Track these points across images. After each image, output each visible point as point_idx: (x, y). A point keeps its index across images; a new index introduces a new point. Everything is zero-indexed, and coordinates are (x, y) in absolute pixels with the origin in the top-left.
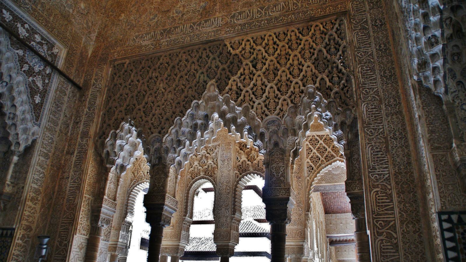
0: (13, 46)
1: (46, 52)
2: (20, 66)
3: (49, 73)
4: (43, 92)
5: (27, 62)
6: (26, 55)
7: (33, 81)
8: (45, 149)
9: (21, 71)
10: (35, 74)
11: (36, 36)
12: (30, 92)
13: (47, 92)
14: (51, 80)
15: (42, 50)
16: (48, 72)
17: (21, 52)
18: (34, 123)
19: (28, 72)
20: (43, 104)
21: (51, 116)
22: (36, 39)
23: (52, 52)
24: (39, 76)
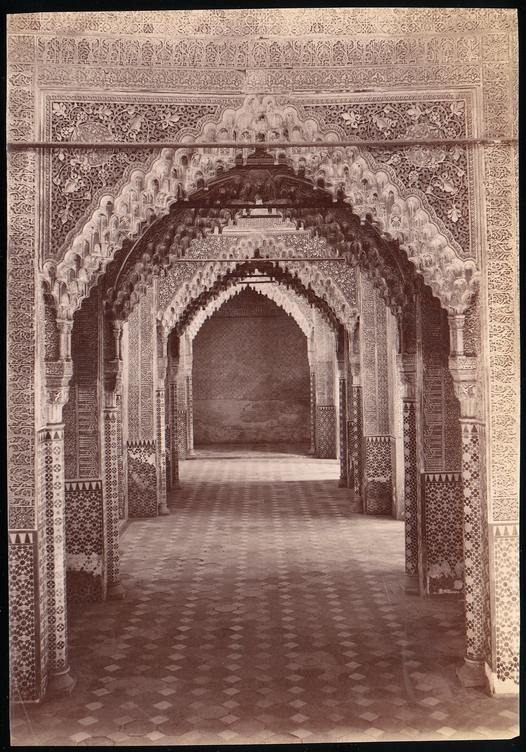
0: (380, 159)
1: (439, 124)
2: (404, 181)
3: (460, 156)
4: (460, 195)
5: (413, 166)
6: (407, 157)
7: (436, 190)
8: (498, 287)
9: (409, 187)
10: (434, 176)
11: (411, 112)
12: (437, 211)
13: (469, 192)
14: (468, 166)
15: (431, 127)
16: (456, 157)
17: (395, 159)
18: (461, 256)
19: (421, 180)
20: (468, 215)
21: (491, 227)
22: (413, 118)
23: (451, 115)
24: (443, 174)
